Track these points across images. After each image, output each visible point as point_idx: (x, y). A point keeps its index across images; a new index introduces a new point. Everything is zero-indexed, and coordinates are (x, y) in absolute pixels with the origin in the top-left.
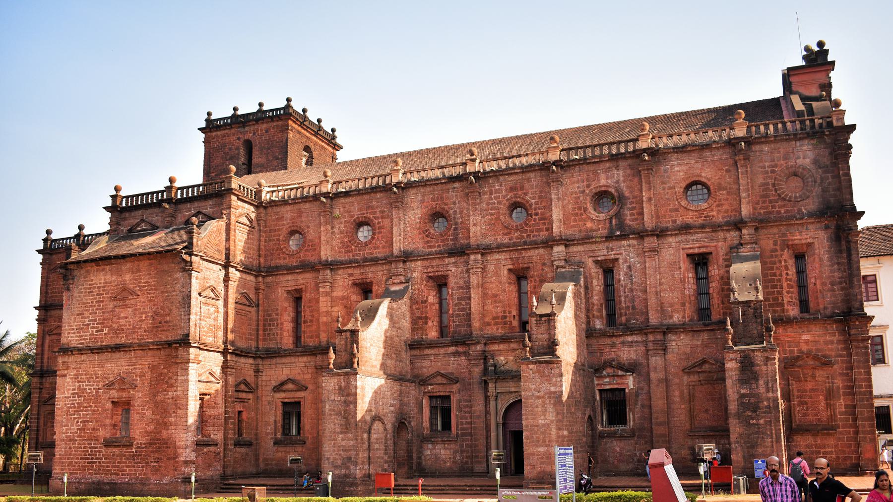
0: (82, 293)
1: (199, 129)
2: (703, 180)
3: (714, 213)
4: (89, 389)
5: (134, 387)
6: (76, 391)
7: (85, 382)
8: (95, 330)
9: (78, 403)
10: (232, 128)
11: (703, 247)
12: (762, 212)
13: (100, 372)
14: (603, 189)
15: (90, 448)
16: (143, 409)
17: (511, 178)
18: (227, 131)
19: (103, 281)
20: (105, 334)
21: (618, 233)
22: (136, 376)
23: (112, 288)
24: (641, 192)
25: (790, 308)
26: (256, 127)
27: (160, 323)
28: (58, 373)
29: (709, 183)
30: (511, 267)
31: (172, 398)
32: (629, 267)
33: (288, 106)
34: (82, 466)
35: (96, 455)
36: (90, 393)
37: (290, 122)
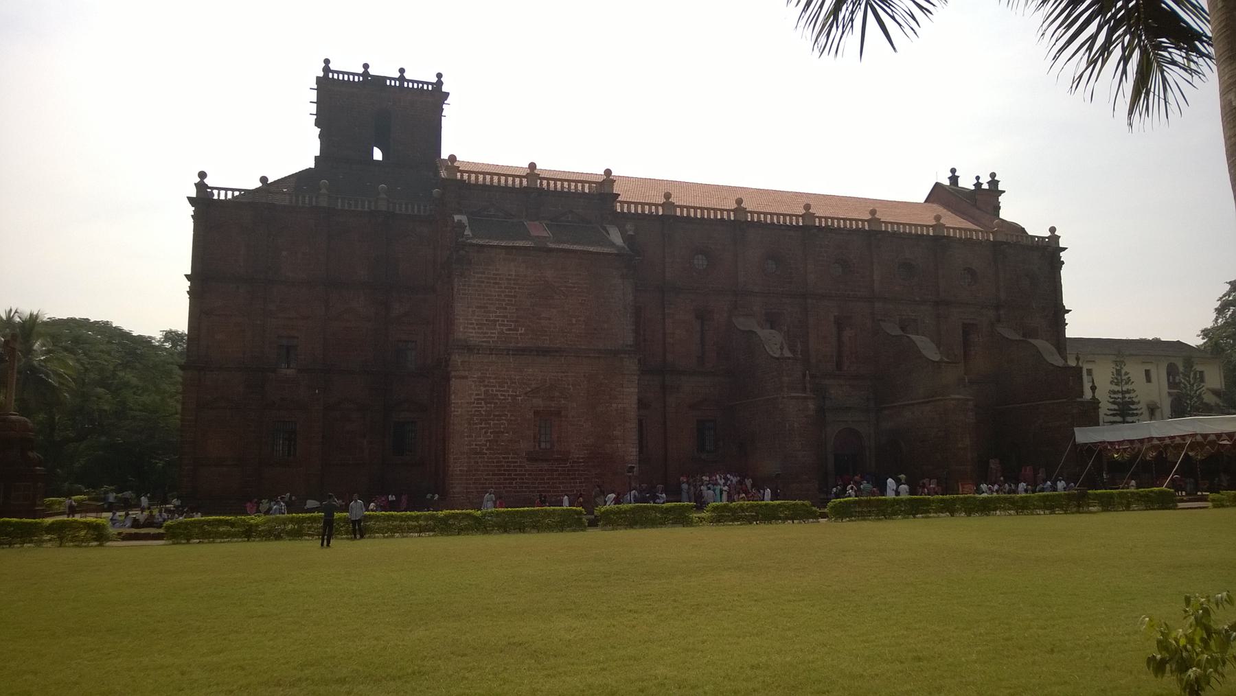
0: (483, 282)
4: (502, 395)
6: (482, 397)
7: (494, 386)
8: (505, 328)
9: (486, 411)
13: (517, 377)
15: (505, 462)
20: (521, 334)
22: (568, 385)
23: (529, 283)
27: (595, 329)
28: (453, 373)
30: (836, 314)
31: (616, 410)
34: (495, 484)
35: (516, 470)
36: (503, 399)
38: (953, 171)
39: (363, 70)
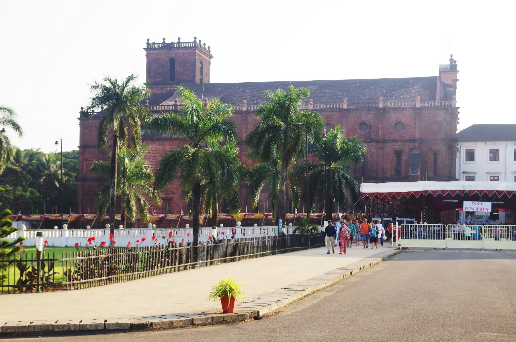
1: (144, 49)
2: (402, 122)
3: (405, 136)
5: (173, 193)
10: (163, 50)
11: (400, 148)
12: (423, 136)
14: (364, 122)
16: (178, 202)
17: (326, 113)
18: (159, 51)
19: (155, 148)
21: (368, 140)
22: (174, 189)
24: (379, 125)
25: (430, 173)
26: (177, 51)
29: (404, 124)
32: (372, 154)
33: (195, 42)
37: (197, 51)
38: (451, 56)
39: (163, 41)
